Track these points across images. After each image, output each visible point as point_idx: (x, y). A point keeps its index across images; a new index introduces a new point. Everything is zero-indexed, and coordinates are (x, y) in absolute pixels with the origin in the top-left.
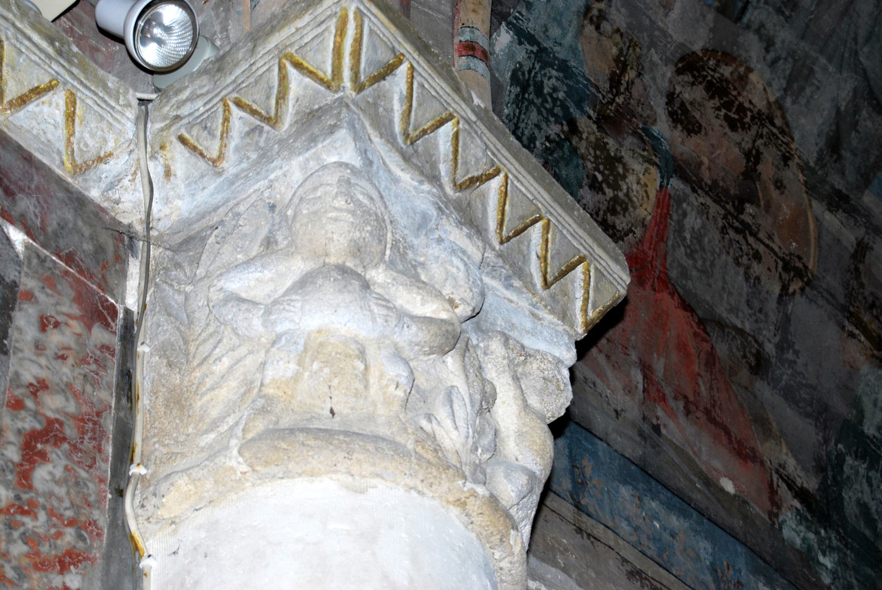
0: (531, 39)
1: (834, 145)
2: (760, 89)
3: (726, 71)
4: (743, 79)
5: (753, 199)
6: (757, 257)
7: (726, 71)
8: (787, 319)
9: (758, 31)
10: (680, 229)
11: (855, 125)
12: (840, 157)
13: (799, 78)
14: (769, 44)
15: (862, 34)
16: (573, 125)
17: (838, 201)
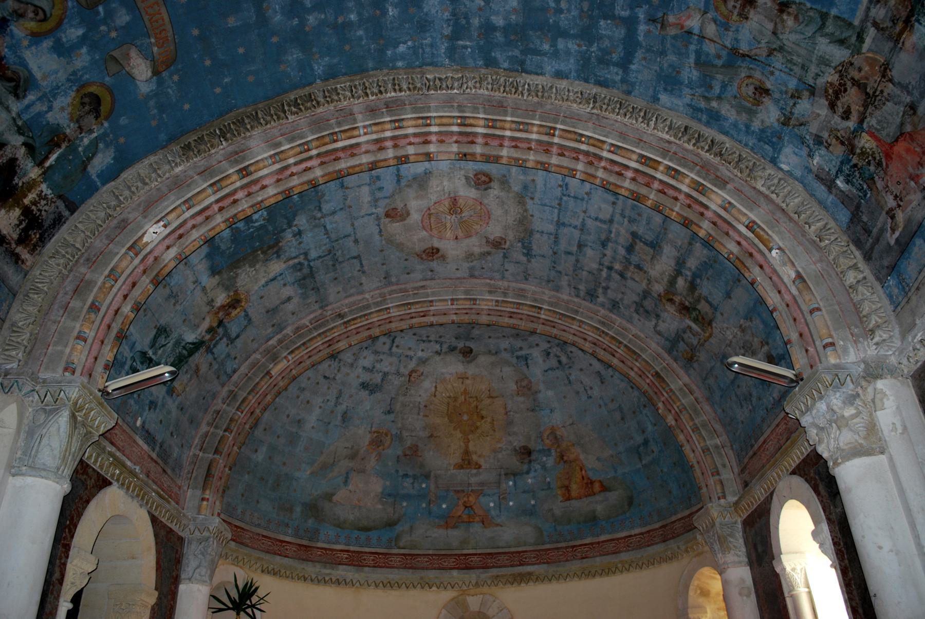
0: (837, 173)
1: (842, 42)
2: (831, 77)
3: (831, 91)
4: (831, 84)
5: (865, 86)
6: (882, 92)
7: (831, 91)
8: (899, 83)
9: (815, 79)
10: (876, 129)
11: (833, 34)
12: (845, 39)
13: (824, 62)
14: (818, 75)
15: (802, 37)
16: (855, 166)
17: (860, 38)
